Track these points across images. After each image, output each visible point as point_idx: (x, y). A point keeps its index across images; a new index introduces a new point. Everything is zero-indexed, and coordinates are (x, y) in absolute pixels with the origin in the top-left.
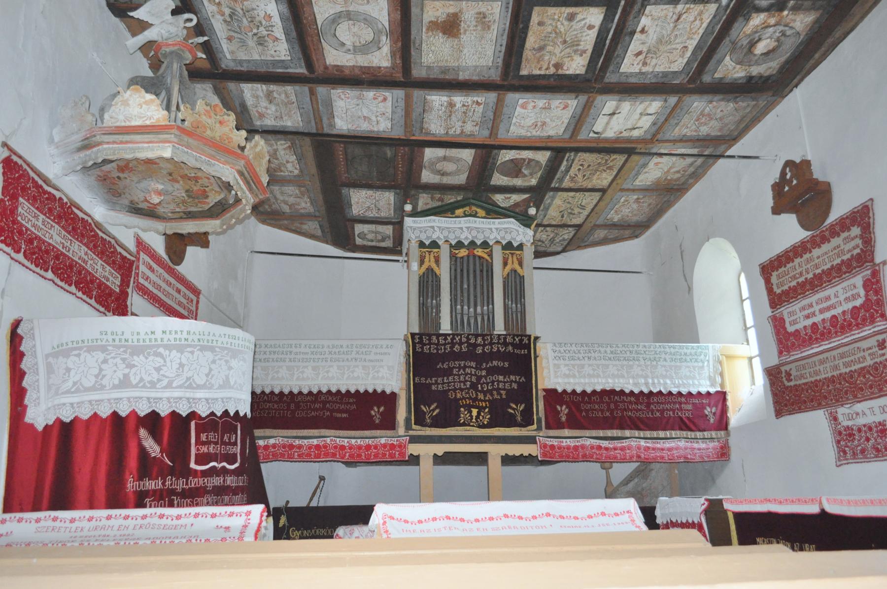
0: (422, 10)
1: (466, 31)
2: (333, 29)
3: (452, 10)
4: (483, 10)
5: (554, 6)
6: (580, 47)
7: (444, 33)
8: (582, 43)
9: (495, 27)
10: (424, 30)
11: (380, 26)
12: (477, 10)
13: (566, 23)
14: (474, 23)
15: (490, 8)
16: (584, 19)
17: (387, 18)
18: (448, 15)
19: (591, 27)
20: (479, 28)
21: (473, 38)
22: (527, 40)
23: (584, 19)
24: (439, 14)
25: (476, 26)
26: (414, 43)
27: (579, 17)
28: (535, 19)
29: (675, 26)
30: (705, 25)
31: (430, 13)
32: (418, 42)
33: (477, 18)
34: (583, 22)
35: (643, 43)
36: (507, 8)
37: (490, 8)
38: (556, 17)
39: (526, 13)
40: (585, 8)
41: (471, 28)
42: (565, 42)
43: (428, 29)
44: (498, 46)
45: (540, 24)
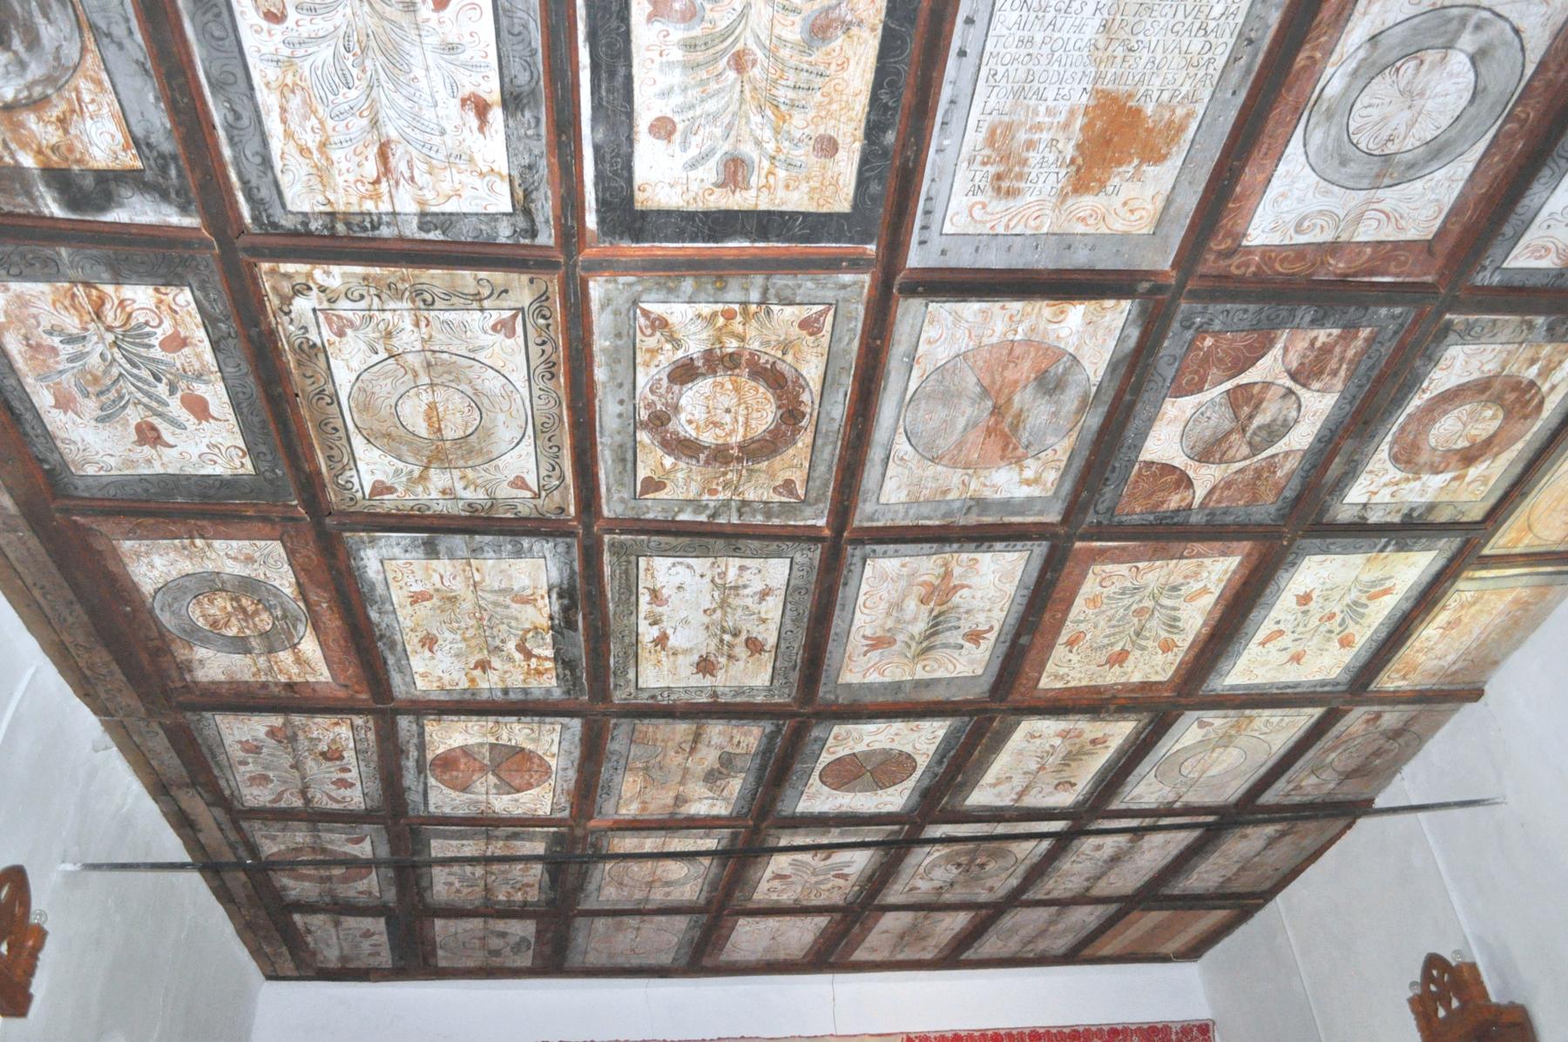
0: (1169, 201)
1: (1066, 126)
2: (1453, 132)
3: (1087, 202)
4: (998, 206)
5: (793, 215)
6: (678, 33)
7: (1138, 112)
8: (677, 54)
9: (974, 138)
10: (1194, 126)
11: (1317, 137)
12: (1015, 204)
13: (748, 150)
14: (1034, 157)
15: (978, 213)
16: (693, 165)
17: (1281, 168)
18: (1102, 185)
19: (664, 128)
20: (1022, 136)
21: (1050, 94)
22: (870, 76)
23: (693, 165)
24: (1129, 190)
25: (1030, 145)
26: (1248, 71)
27: (709, 172)
28: (846, 166)
29: (375, 123)
30: (276, 146)
31: (1150, 192)
32: (1234, 77)
33: (1020, 177)
34: (693, 152)
35: (451, 48)
36: (927, 213)
37: (977, 212)
38: (782, 173)
39: (875, 188)
40: (699, 206)
41: (1045, 136)
42: (740, 62)
43: (1181, 129)
44: (972, 51)
45: (828, 147)
